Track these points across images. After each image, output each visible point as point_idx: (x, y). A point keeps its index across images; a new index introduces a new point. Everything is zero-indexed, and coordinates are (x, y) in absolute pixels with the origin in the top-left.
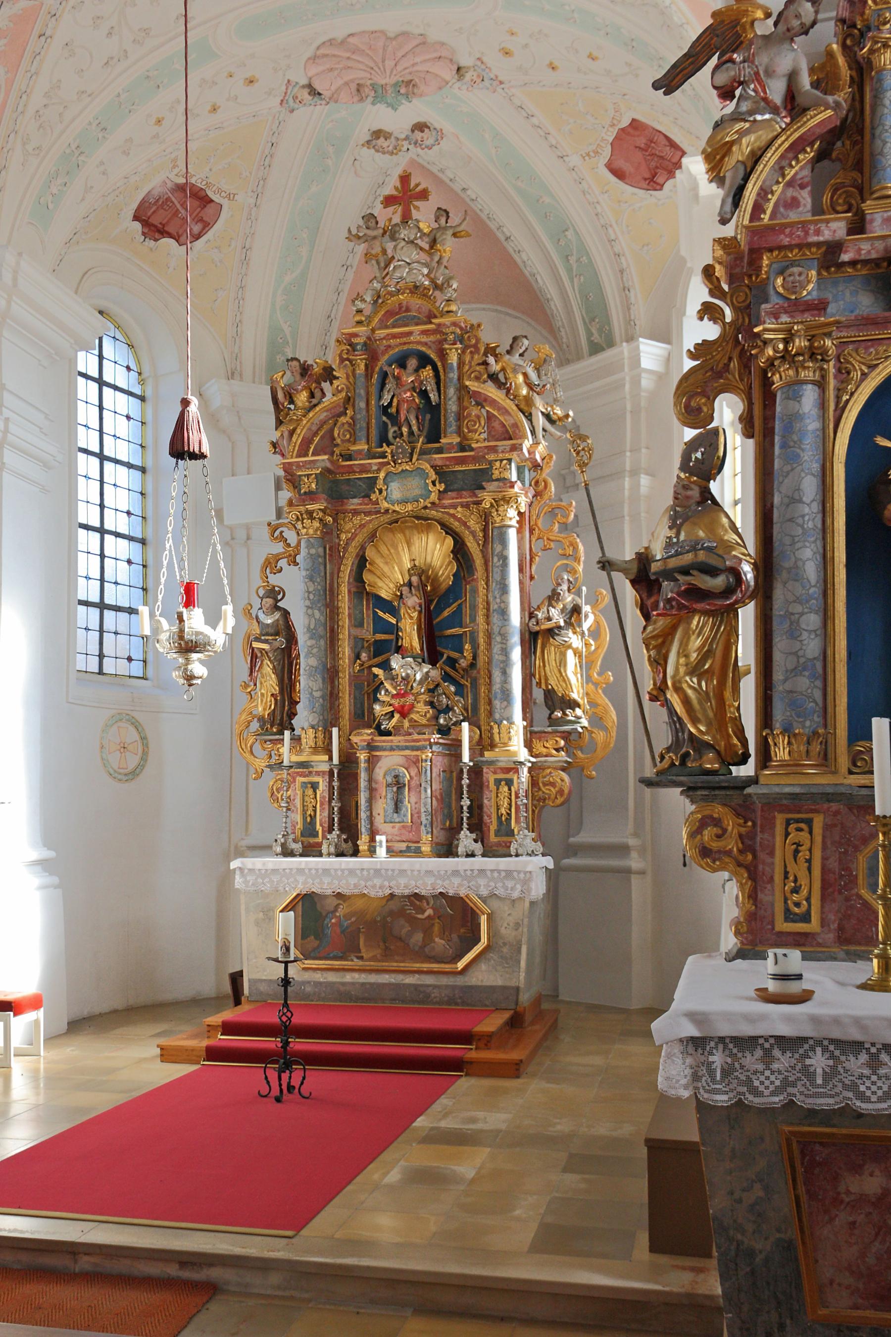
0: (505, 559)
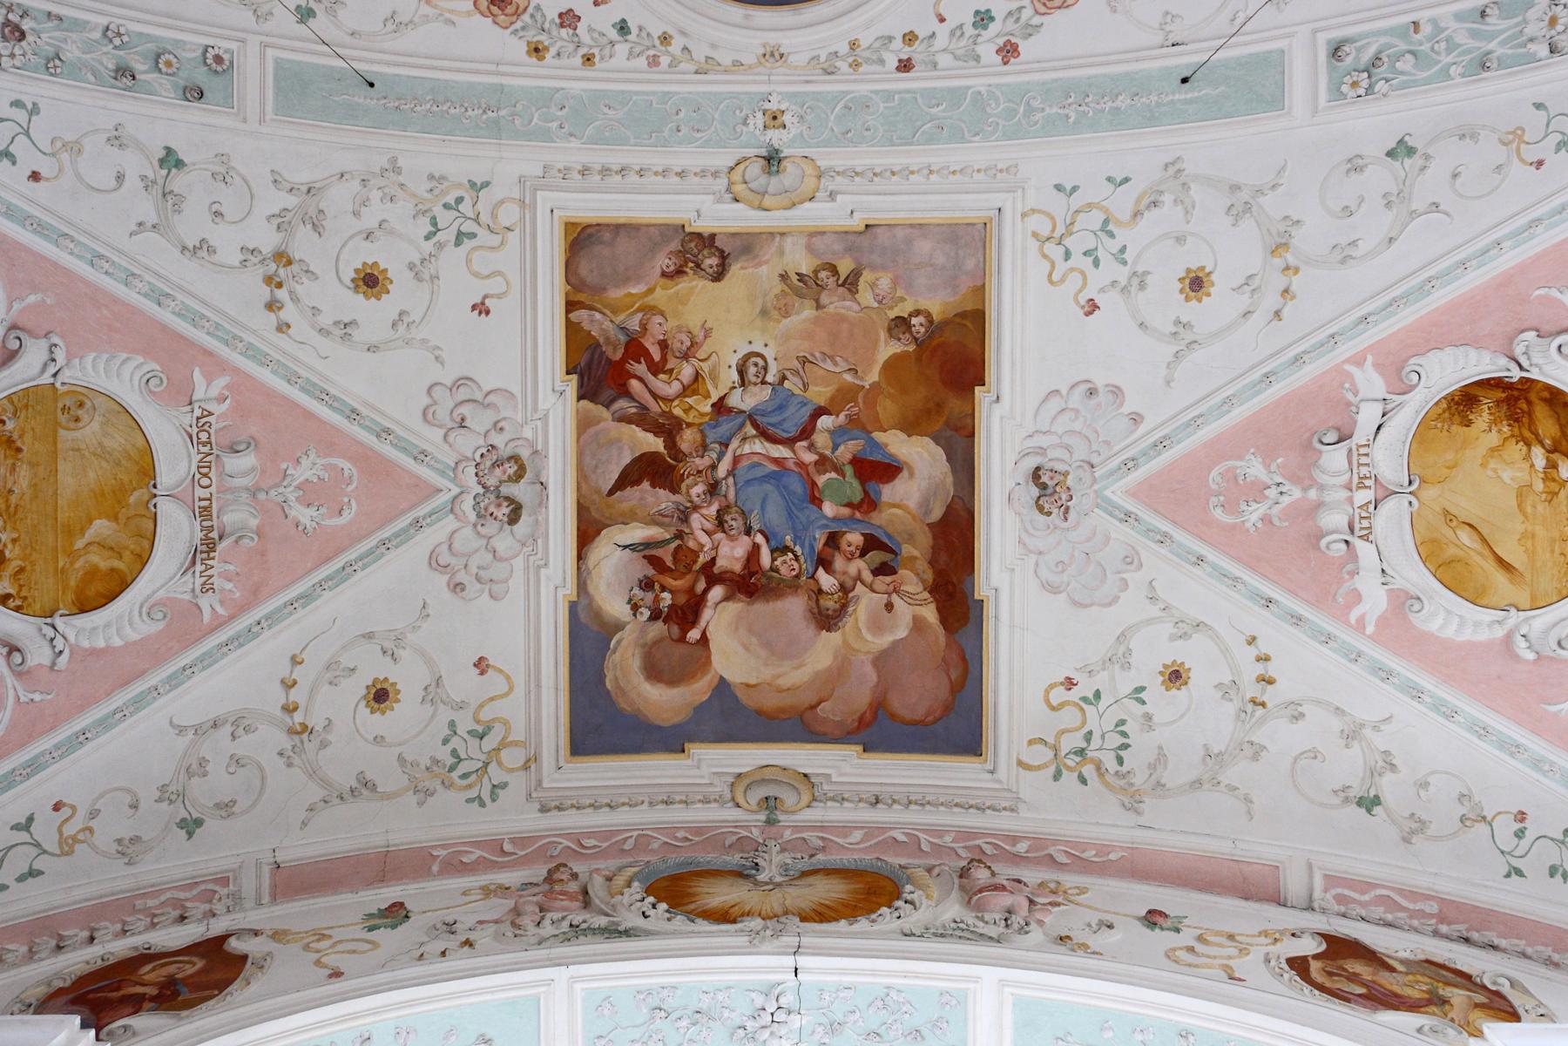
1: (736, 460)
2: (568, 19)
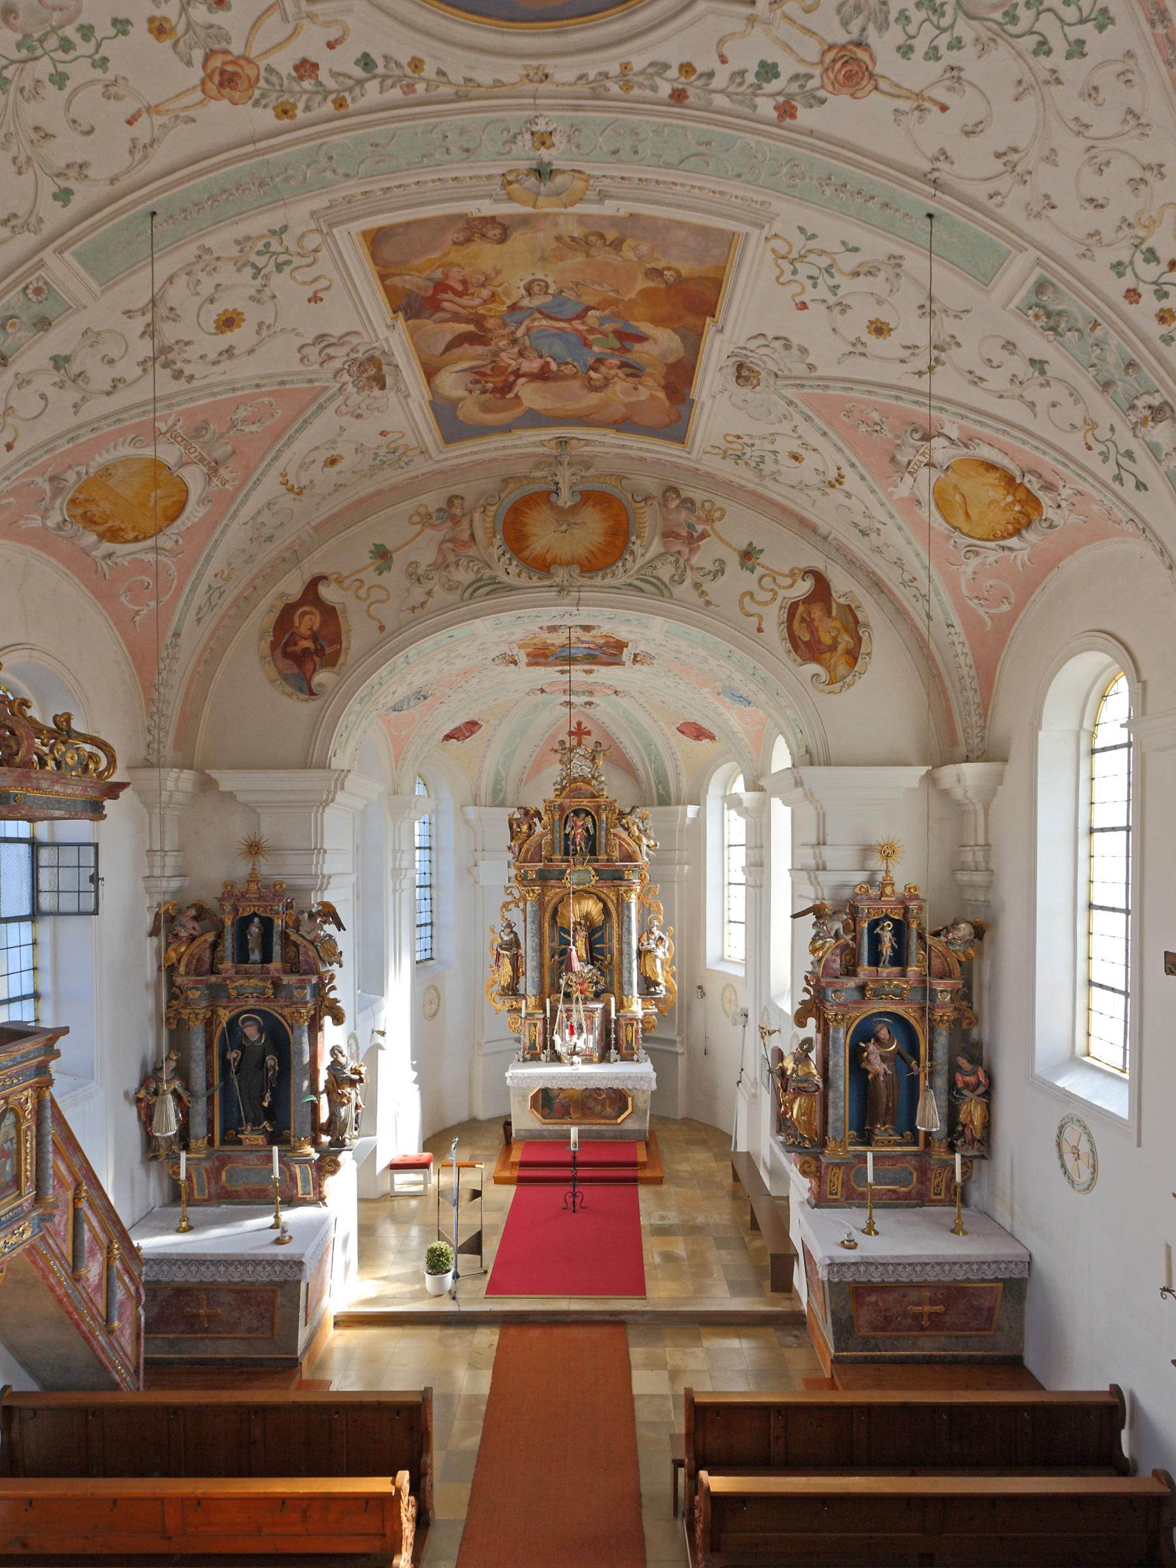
0: (629, 918)
1: (528, 329)
2: (306, 68)
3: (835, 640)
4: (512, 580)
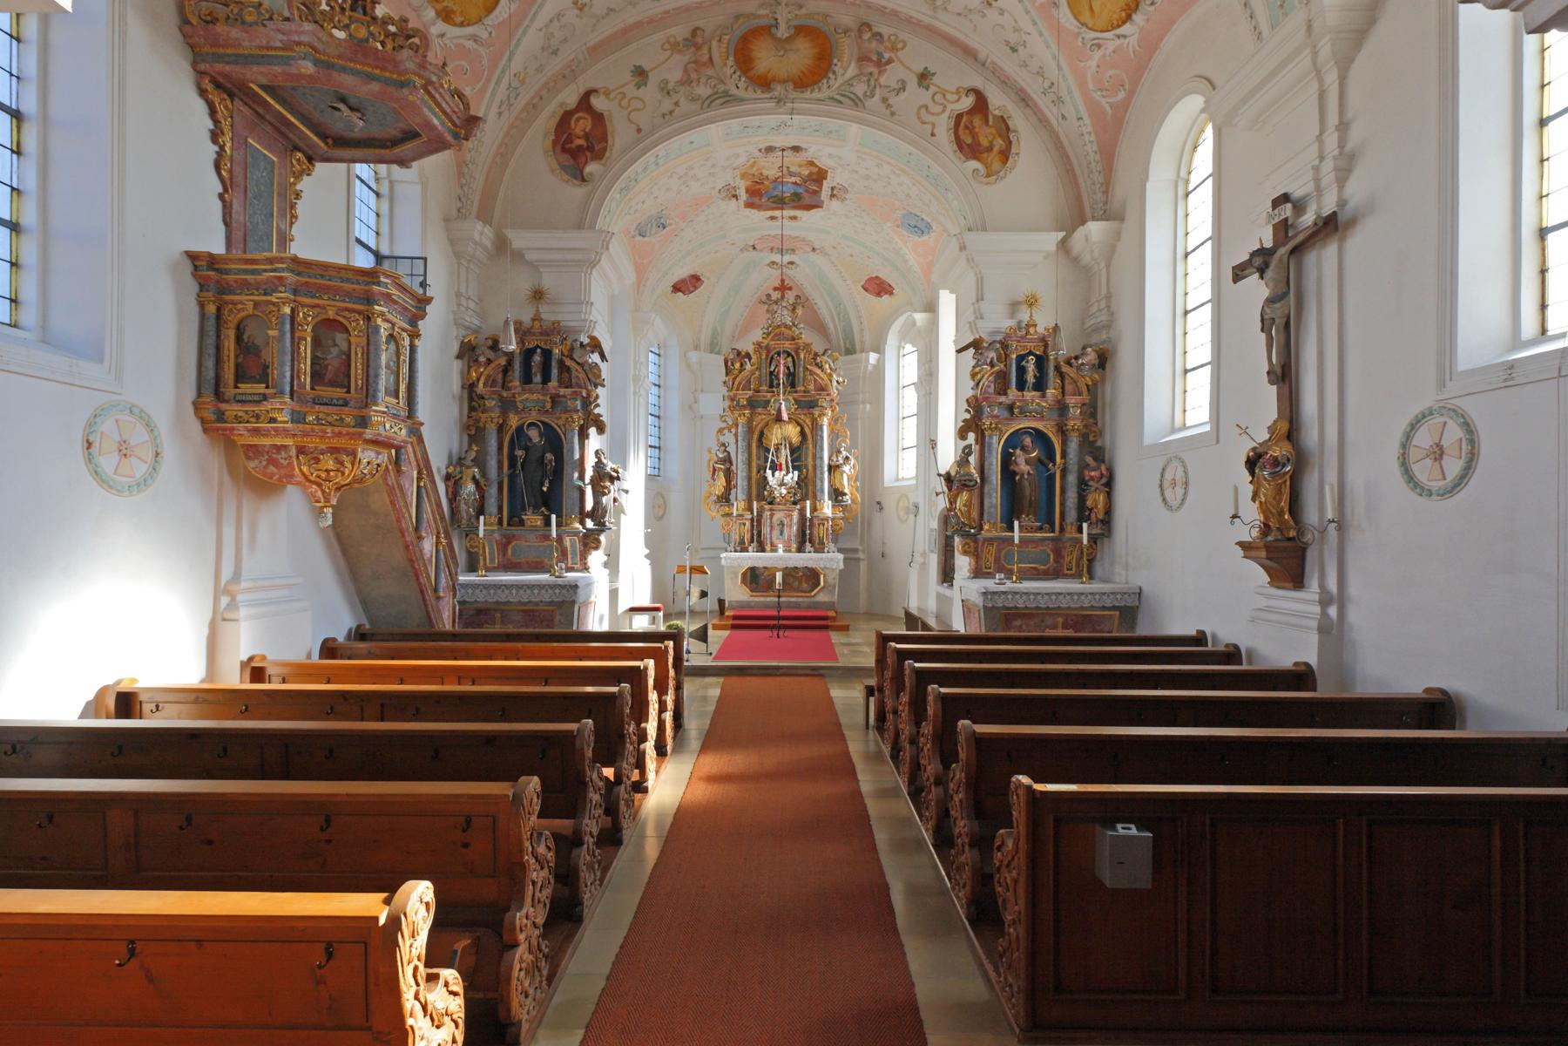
3: (991, 143)
4: (741, 93)
